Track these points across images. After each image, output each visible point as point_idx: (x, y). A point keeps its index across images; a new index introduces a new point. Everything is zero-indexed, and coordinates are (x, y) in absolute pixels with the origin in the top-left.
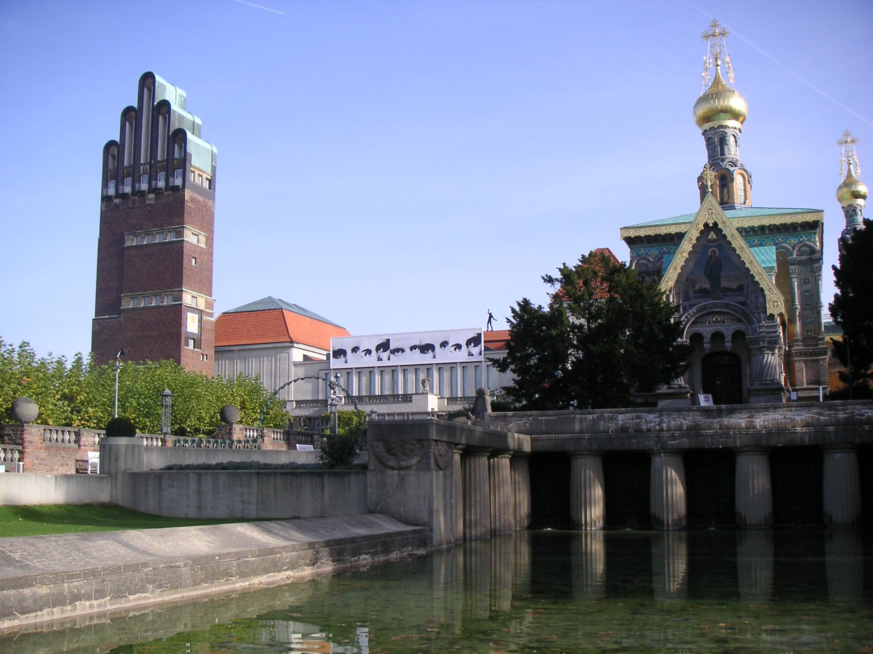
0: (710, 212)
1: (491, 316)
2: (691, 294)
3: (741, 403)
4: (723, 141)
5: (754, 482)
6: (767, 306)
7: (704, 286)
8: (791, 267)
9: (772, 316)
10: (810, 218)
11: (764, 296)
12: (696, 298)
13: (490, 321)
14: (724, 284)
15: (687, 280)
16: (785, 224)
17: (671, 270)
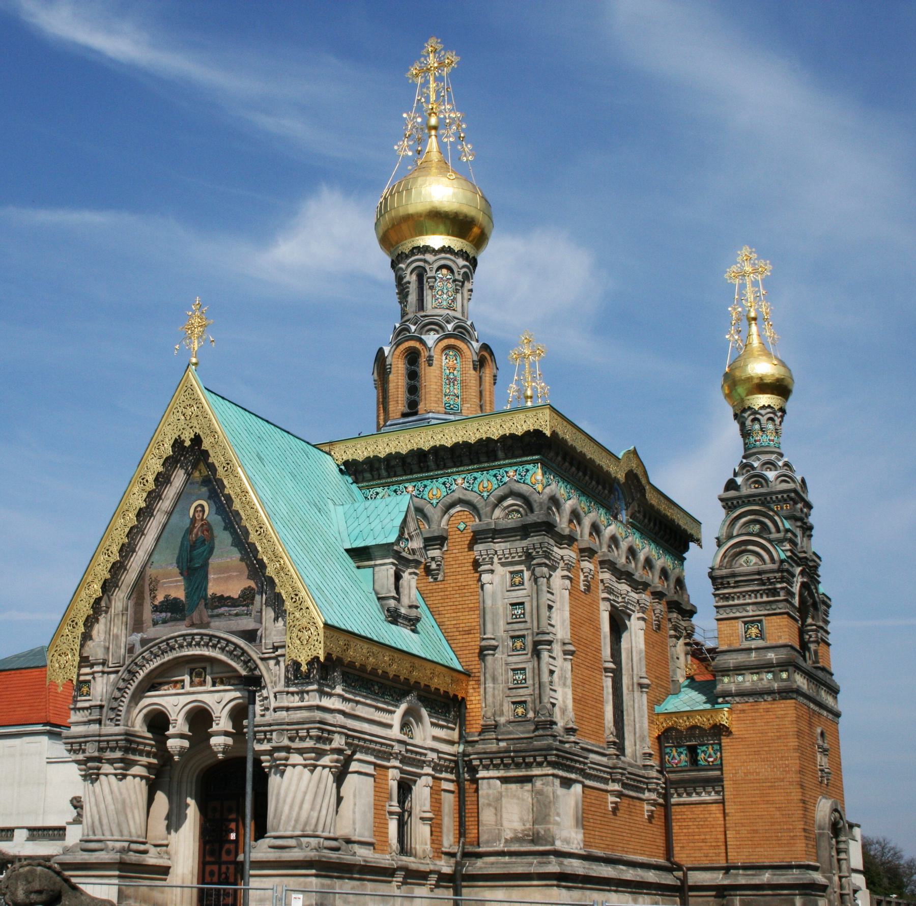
2: (148, 614)
12: (155, 623)
14: (214, 588)
16: (466, 444)
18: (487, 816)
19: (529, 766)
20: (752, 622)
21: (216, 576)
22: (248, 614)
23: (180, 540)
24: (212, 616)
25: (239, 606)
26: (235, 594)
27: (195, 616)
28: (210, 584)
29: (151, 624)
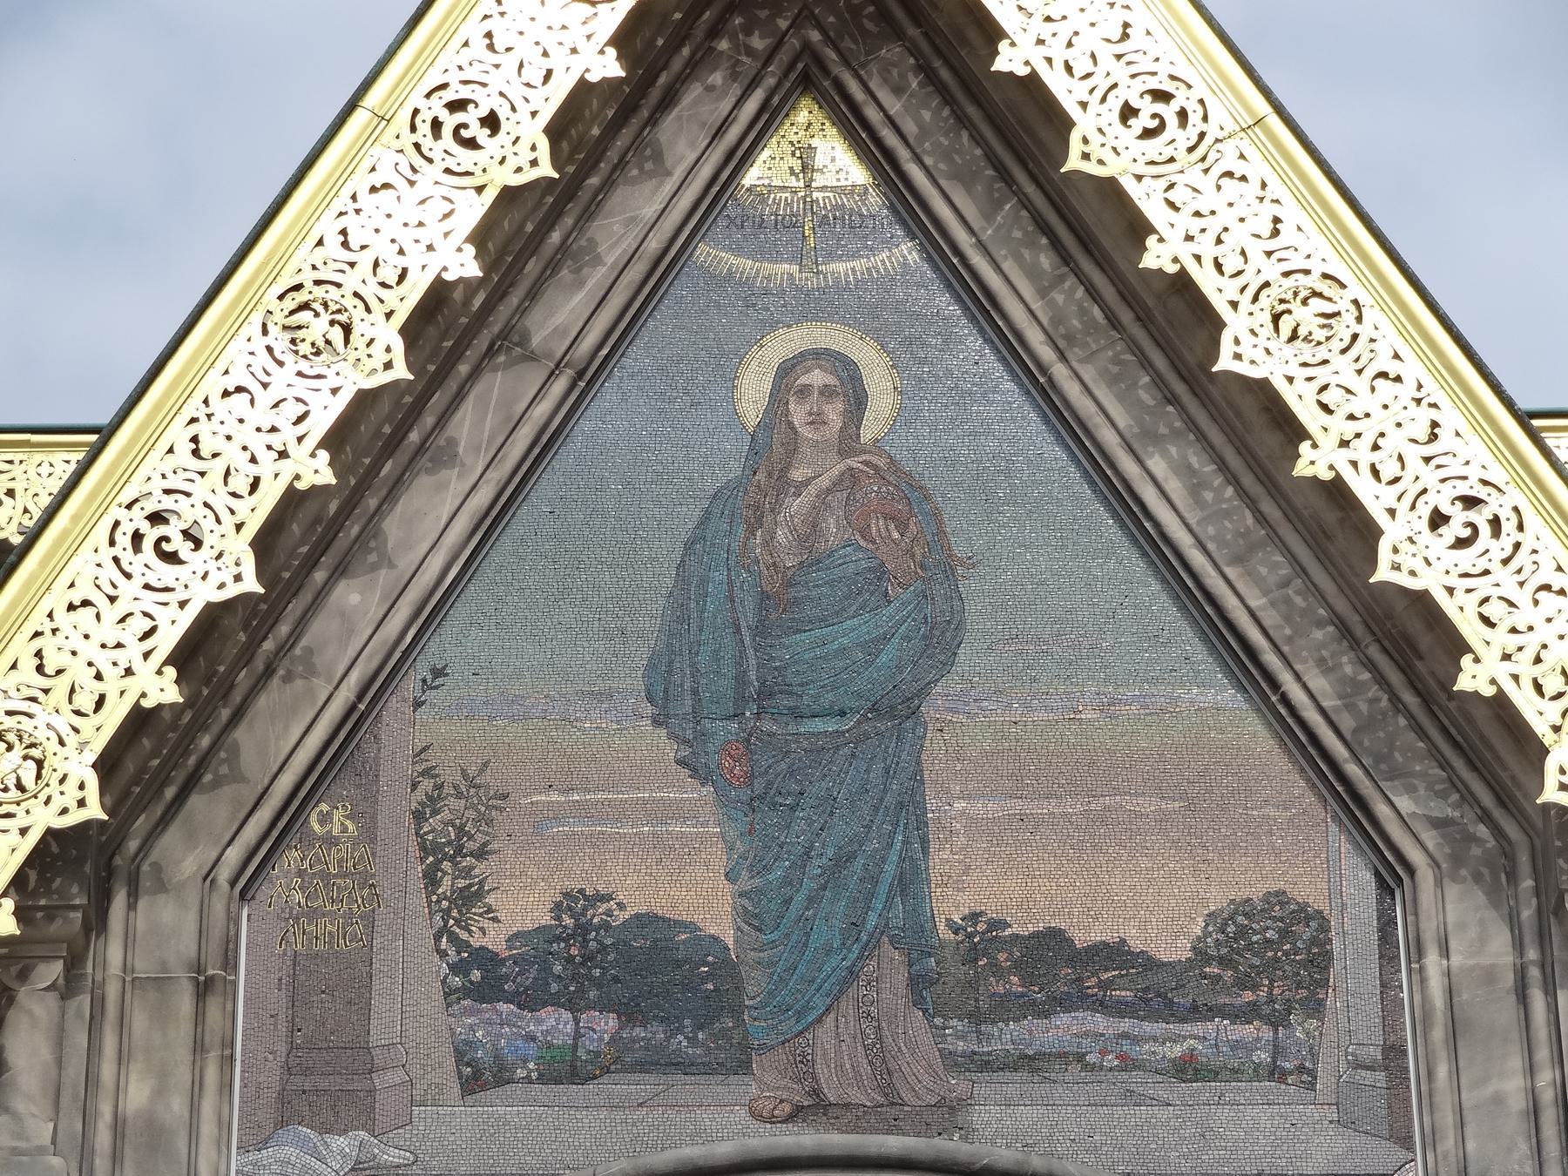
2: (411, 1005)
7: (635, 890)
12: (479, 1076)
21: (978, 808)
23: (668, 550)
24: (986, 1065)
25: (1196, 1012)
26: (1170, 939)
27: (836, 1049)
28: (941, 859)
29: (447, 1074)
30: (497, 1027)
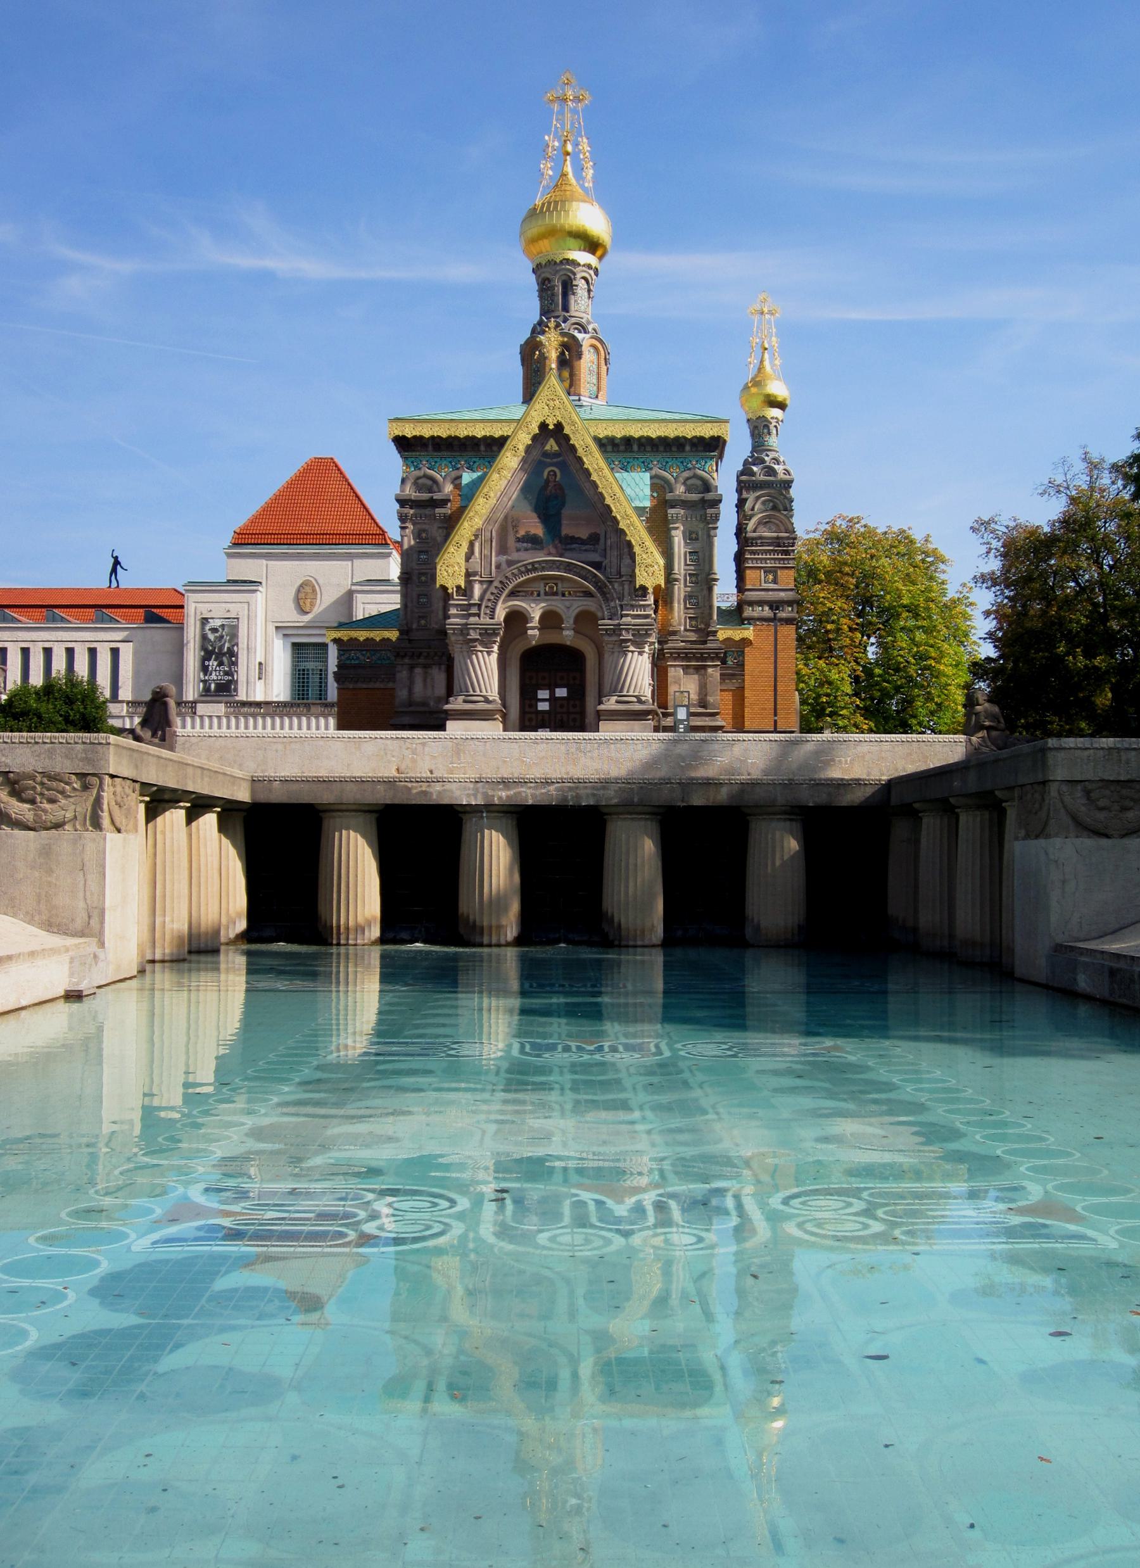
0: (551, 403)
1: (117, 562)
2: (511, 542)
3: (582, 728)
4: (568, 287)
5: (637, 866)
6: (637, 571)
7: (533, 531)
8: (671, 511)
9: (644, 589)
10: (707, 431)
11: (632, 556)
12: (518, 550)
13: (114, 571)
14: (566, 530)
15: (506, 517)
16: (666, 438)
17: (481, 500)
18: (672, 688)
19: (705, 660)
20: (770, 572)
22: (595, 551)
24: (566, 550)
28: (563, 527)
30: (519, 545)
